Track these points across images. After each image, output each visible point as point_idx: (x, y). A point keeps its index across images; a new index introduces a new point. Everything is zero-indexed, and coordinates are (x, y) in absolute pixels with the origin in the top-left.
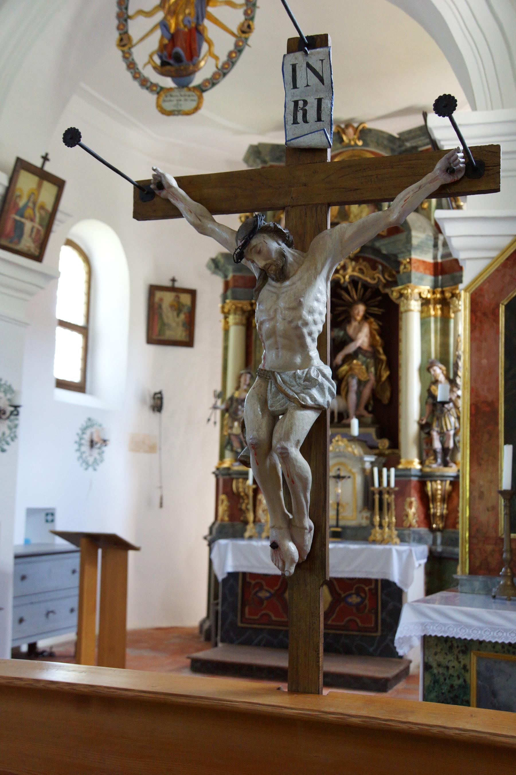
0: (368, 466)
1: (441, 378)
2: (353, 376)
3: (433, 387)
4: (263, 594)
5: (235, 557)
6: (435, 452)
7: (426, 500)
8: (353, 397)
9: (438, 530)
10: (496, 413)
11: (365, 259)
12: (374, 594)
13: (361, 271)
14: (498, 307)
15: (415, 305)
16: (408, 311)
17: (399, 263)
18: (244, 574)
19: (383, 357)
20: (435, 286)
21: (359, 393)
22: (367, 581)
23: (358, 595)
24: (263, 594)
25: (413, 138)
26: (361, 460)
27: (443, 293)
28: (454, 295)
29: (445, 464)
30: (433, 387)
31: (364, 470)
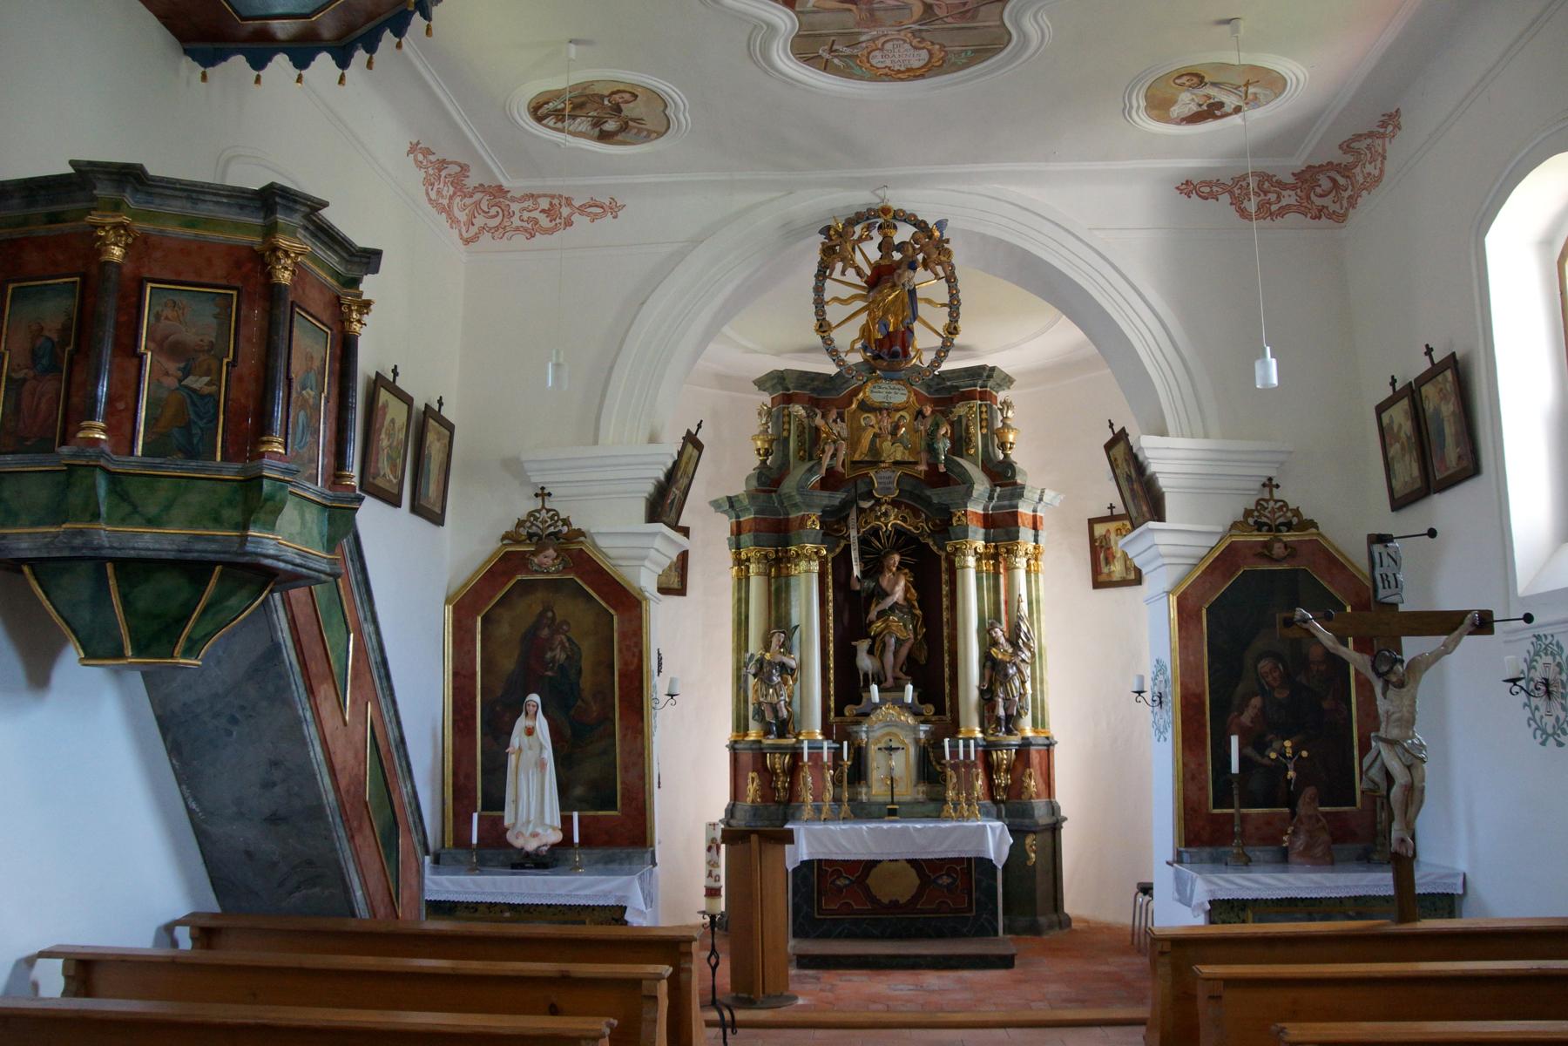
0: (922, 735)
1: (1002, 640)
2: (891, 634)
3: (994, 651)
4: (841, 882)
5: (809, 844)
6: (998, 719)
7: (990, 769)
8: (889, 657)
9: (1002, 801)
10: (1203, 704)
11: (907, 506)
12: (967, 873)
13: (904, 519)
14: (1200, 610)
15: (971, 561)
16: (964, 567)
17: (951, 515)
18: (820, 861)
19: (918, 612)
20: (987, 540)
21: (896, 654)
22: (959, 860)
23: (948, 875)
24: (841, 882)
25: (958, 378)
26: (915, 730)
27: (996, 547)
28: (1008, 552)
29: (1009, 732)
30: (994, 651)
31: (917, 741)
